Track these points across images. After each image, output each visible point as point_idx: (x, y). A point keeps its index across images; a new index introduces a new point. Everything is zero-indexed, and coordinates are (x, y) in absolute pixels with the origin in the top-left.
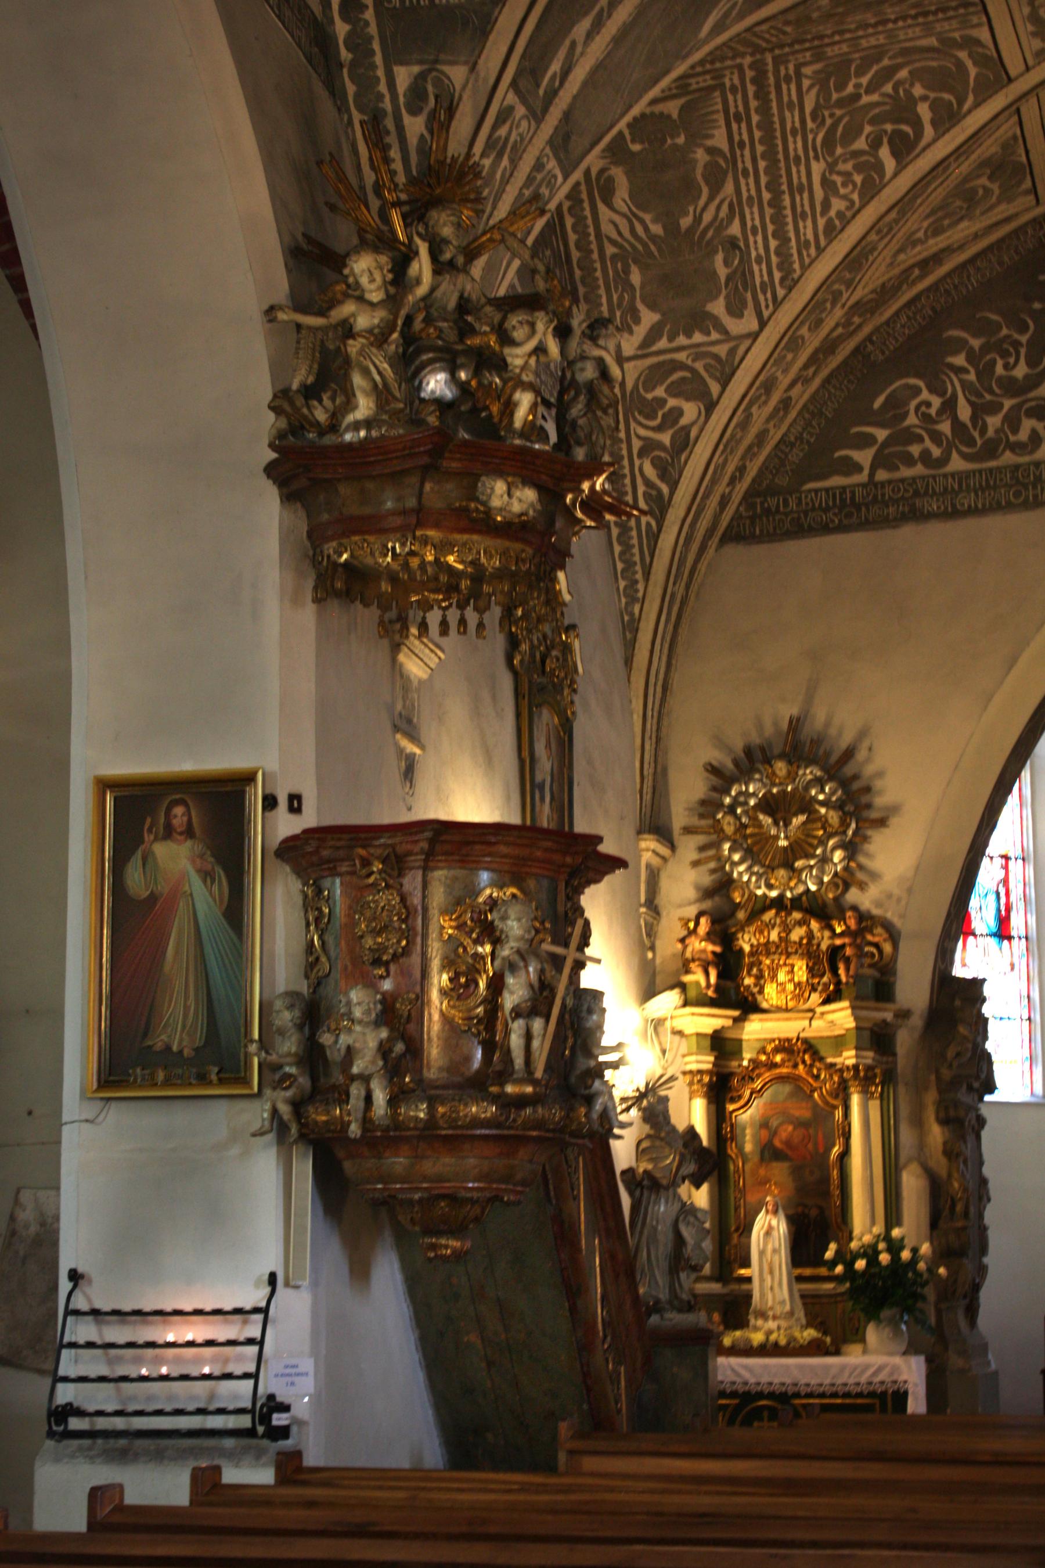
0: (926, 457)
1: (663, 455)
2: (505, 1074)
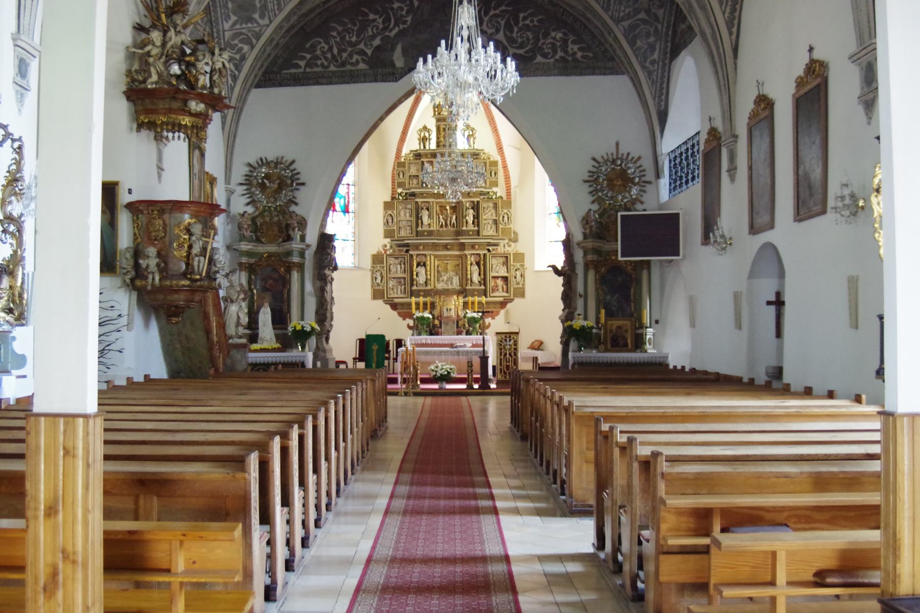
0: (322, 65)
1: (236, 62)
2: (192, 273)
